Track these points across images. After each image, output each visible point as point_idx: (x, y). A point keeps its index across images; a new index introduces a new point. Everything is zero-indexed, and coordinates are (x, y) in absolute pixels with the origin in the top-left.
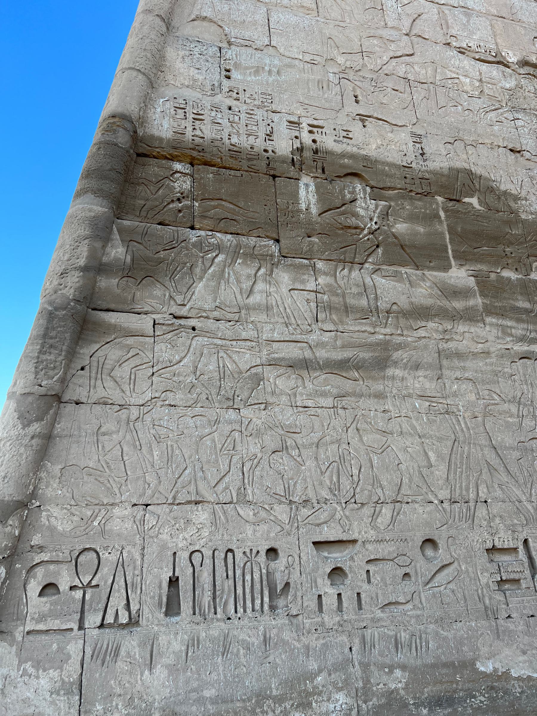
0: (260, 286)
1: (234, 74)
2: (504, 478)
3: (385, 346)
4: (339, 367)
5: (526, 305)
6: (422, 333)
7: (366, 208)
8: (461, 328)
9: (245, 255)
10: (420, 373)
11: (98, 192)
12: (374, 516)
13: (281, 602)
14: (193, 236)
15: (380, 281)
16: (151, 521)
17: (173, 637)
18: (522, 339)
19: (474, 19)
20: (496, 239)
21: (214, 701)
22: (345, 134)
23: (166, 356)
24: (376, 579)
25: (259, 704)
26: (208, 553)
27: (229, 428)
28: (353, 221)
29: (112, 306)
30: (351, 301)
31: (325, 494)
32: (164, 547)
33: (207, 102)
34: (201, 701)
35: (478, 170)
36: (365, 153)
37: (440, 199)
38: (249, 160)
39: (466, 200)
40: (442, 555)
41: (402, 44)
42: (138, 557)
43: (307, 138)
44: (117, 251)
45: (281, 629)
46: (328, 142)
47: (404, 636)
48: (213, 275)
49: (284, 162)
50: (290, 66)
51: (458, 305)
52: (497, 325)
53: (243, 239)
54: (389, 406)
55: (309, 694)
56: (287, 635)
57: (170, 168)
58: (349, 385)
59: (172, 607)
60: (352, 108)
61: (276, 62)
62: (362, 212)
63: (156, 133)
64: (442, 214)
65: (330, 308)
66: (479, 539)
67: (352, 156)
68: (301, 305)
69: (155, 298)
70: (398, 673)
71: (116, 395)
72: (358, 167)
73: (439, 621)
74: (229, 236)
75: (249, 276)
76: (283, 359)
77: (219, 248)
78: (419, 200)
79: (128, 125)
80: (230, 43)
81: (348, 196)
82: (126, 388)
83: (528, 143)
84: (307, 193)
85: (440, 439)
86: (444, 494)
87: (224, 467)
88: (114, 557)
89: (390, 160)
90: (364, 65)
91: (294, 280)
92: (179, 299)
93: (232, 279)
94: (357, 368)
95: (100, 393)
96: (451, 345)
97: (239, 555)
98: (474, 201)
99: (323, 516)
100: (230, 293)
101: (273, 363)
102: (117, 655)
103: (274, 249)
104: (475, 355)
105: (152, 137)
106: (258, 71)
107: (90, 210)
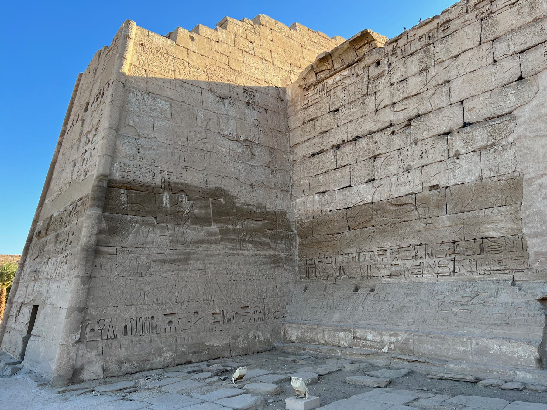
0: (150, 235)
1: (142, 151)
2: (219, 293)
3: (189, 254)
4: (174, 261)
5: (234, 237)
6: (200, 249)
7: (186, 204)
8: (213, 246)
9: (145, 224)
10: (199, 262)
11: (99, 206)
12: (181, 306)
13: (154, 331)
14: (128, 218)
15: (189, 231)
16: (119, 311)
17: (126, 341)
18: (231, 249)
19: (230, 121)
20: (227, 214)
21: (137, 355)
22: (179, 175)
23: (121, 261)
24: (181, 323)
25: (149, 355)
26: (135, 319)
27: (140, 283)
28: (181, 209)
29: (103, 245)
30: (179, 239)
31: (168, 301)
32: (123, 318)
33: (132, 164)
34: (134, 355)
35: (224, 188)
36: (186, 182)
37: (210, 199)
38: (147, 187)
39: (219, 199)
40: (199, 316)
41: (202, 134)
42: (116, 320)
43: (166, 177)
44: (104, 225)
45: (155, 337)
46: (174, 179)
47: (187, 337)
48: (135, 232)
49: (158, 188)
50: (161, 146)
51: (212, 238)
52: (224, 245)
53: (145, 218)
54: (188, 273)
55: (161, 352)
56: (156, 339)
57: (119, 192)
58: (177, 267)
59: (126, 333)
60: (183, 164)
61: (156, 145)
62: (184, 206)
63: (114, 178)
64: (211, 205)
65: (172, 241)
66: (210, 311)
67: (182, 184)
68: (163, 240)
69: (116, 242)
70: (185, 346)
71: (106, 274)
72: (184, 188)
73: (197, 333)
74: (140, 217)
75: (146, 232)
76: (157, 260)
77: (137, 222)
78: (204, 200)
79: (107, 179)
80: (139, 136)
81: (180, 200)
82: (109, 271)
83: (243, 176)
84: (166, 200)
85: (202, 283)
86: (202, 299)
87: (139, 294)
88: (109, 321)
89: (195, 185)
90: (188, 144)
91: (161, 232)
92: (124, 241)
93: (141, 233)
94: (180, 261)
95: (102, 274)
96: (209, 252)
97: (143, 319)
98: (222, 200)
99: (167, 307)
100: (140, 238)
101: (154, 261)
102: (112, 345)
103: (155, 221)
104: (216, 255)
105: (113, 180)
106: (150, 149)
107: (97, 213)
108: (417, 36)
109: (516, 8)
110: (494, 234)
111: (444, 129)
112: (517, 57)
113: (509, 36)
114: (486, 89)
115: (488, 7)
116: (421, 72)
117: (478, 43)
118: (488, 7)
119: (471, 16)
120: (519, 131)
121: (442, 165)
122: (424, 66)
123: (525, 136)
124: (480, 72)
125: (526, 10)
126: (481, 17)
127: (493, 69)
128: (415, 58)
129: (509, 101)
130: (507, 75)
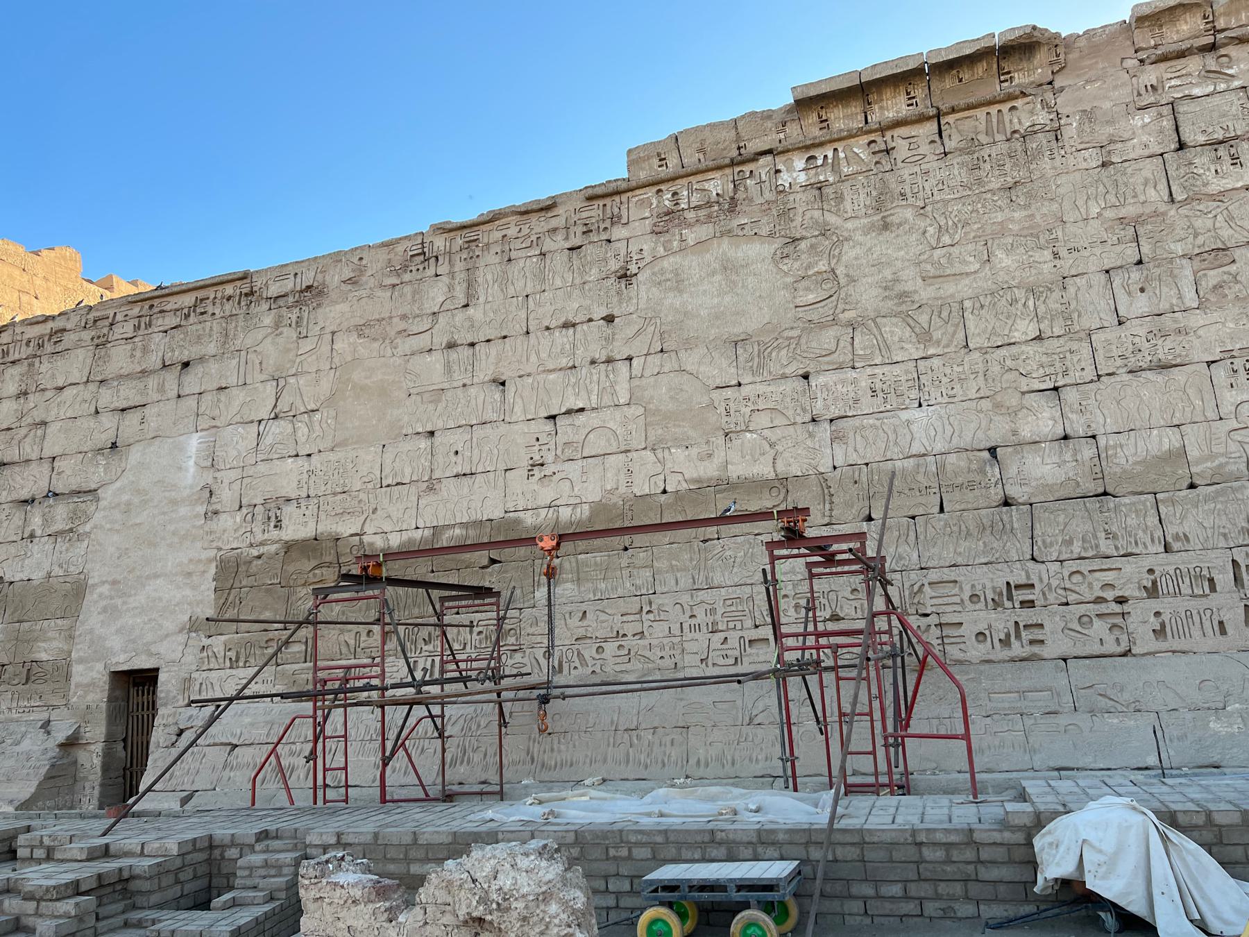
108: (26, 337)
109: (129, 347)
110: (43, 656)
111: (25, 494)
112: (117, 415)
113: (116, 383)
114: (81, 449)
115: (105, 330)
116: (18, 397)
117: (85, 379)
118: (105, 330)
119: (87, 335)
120: (98, 518)
121: (12, 549)
122: (24, 387)
123: (102, 527)
124: (78, 422)
125: (138, 354)
126: (96, 341)
127: (92, 423)
128: (15, 371)
129: (95, 475)
130: (104, 437)
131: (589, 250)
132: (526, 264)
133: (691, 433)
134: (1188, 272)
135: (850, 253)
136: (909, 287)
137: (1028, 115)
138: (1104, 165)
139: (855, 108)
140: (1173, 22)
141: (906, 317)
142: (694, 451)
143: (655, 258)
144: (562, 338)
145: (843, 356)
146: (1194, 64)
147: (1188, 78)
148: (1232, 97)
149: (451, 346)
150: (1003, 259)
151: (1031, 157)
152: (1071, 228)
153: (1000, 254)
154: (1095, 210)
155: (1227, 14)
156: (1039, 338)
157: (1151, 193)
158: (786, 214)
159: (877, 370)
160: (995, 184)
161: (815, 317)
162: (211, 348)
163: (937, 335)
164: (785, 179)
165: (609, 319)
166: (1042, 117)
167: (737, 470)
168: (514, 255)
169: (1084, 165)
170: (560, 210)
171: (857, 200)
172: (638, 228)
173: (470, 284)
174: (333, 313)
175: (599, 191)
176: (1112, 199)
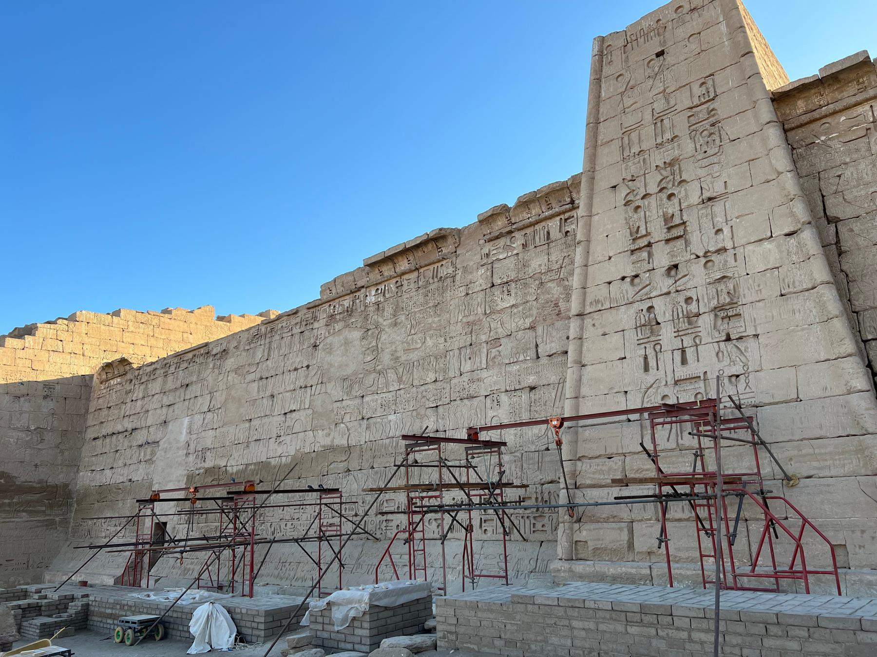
131: (306, 333)
132: (287, 340)
133: (326, 423)
134: (485, 350)
135: (384, 337)
136: (399, 354)
137: (446, 270)
138: (467, 294)
139: (390, 266)
140: (494, 221)
141: (395, 368)
142: (325, 432)
143: (325, 338)
144: (293, 375)
145: (374, 388)
146: (502, 242)
147: (497, 250)
148: (512, 259)
149: (261, 378)
150: (430, 342)
151: (444, 290)
152: (452, 327)
153: (428, 339)
154: (460, 318)
155: (514, 216)
156: (436, 381)
157: (479, 309)
158: (366, 318)
159: (384, 395)
160: (431, 305)
161: (368, 368)
162: (194, 379)
163: (404, 378)
164: (368, 299)
165: (308, 367)
166: (450, 270)
167: (337, 442)
168: (284, 335)
169: (460, 295)
170: (299, 314)
171: (389, 310)
172: (322, 322)
173: (270, 348)
174: (230, 363)
175: (310, 306)
176: (466, 312)
